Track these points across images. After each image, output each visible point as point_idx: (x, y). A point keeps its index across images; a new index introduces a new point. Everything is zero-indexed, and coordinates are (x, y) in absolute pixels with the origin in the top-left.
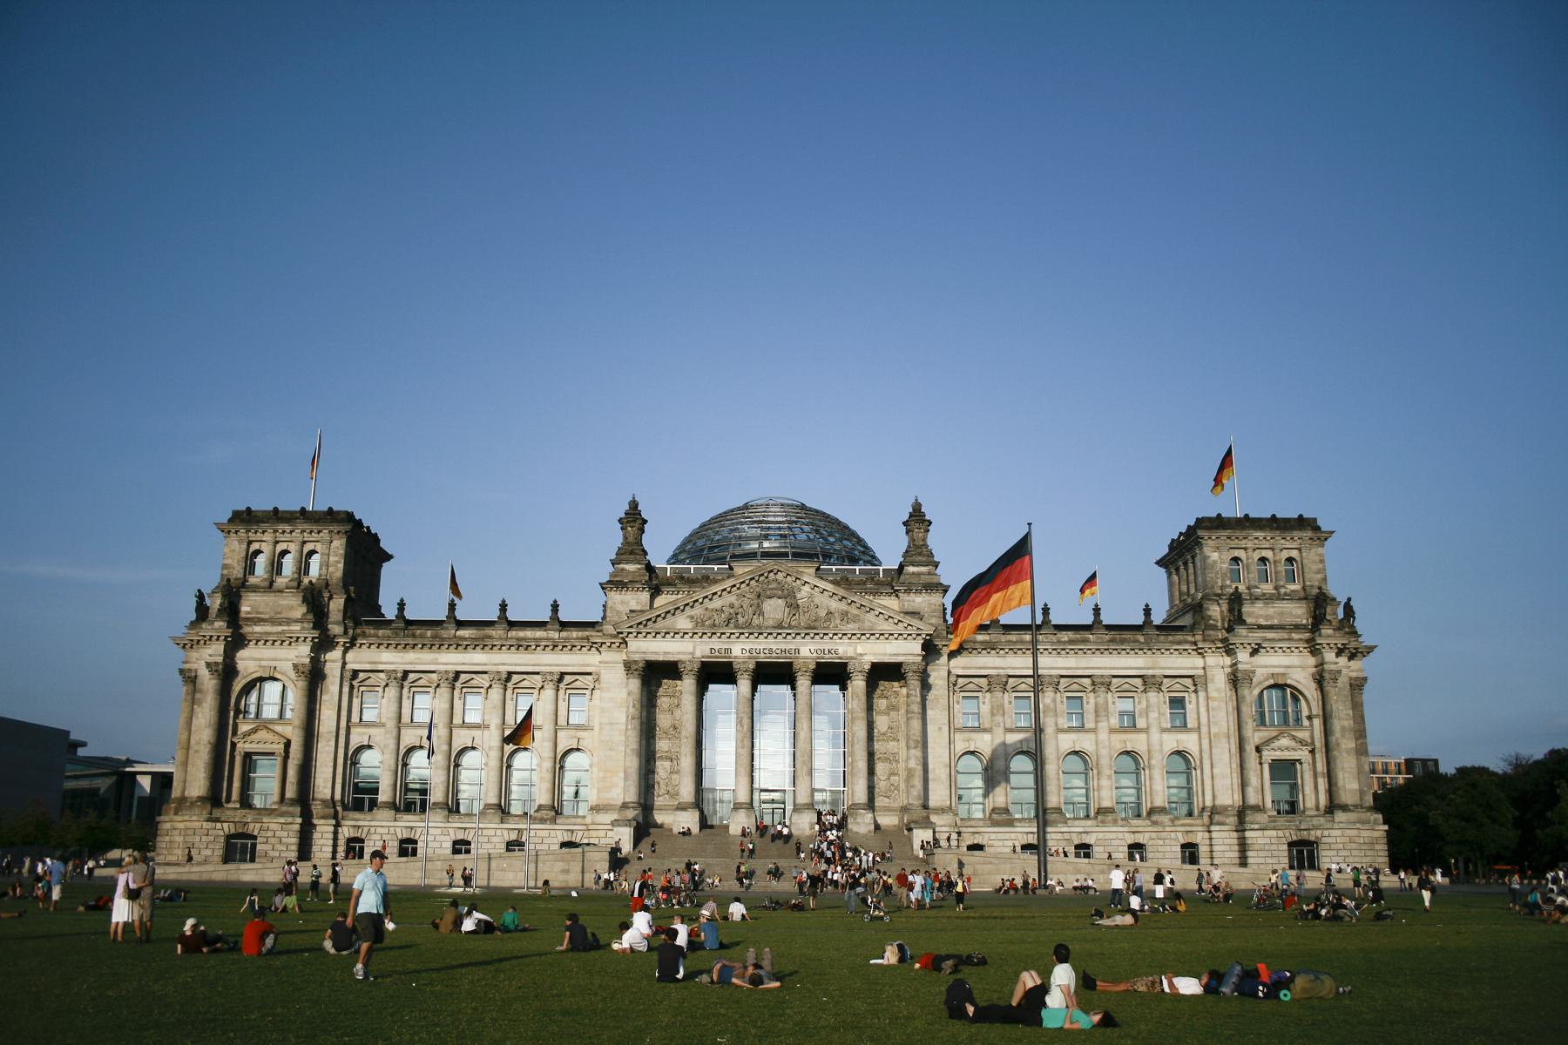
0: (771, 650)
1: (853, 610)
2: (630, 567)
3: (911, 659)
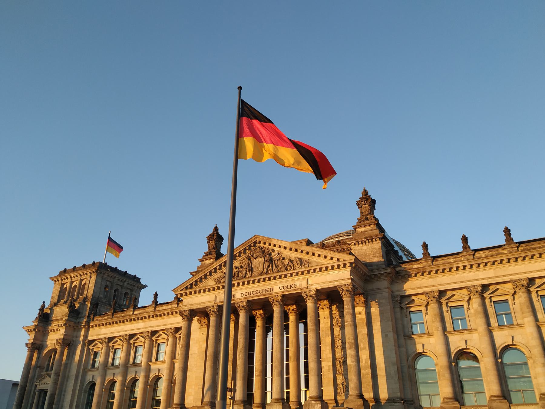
0: (257, 292)
1: (304, 257)
2: (208, 262)
3: (343, 283)
